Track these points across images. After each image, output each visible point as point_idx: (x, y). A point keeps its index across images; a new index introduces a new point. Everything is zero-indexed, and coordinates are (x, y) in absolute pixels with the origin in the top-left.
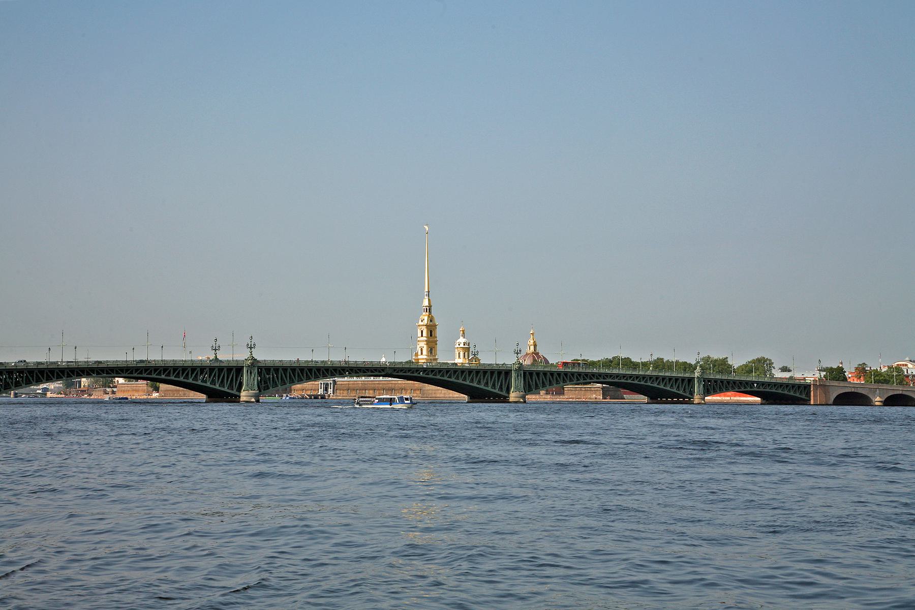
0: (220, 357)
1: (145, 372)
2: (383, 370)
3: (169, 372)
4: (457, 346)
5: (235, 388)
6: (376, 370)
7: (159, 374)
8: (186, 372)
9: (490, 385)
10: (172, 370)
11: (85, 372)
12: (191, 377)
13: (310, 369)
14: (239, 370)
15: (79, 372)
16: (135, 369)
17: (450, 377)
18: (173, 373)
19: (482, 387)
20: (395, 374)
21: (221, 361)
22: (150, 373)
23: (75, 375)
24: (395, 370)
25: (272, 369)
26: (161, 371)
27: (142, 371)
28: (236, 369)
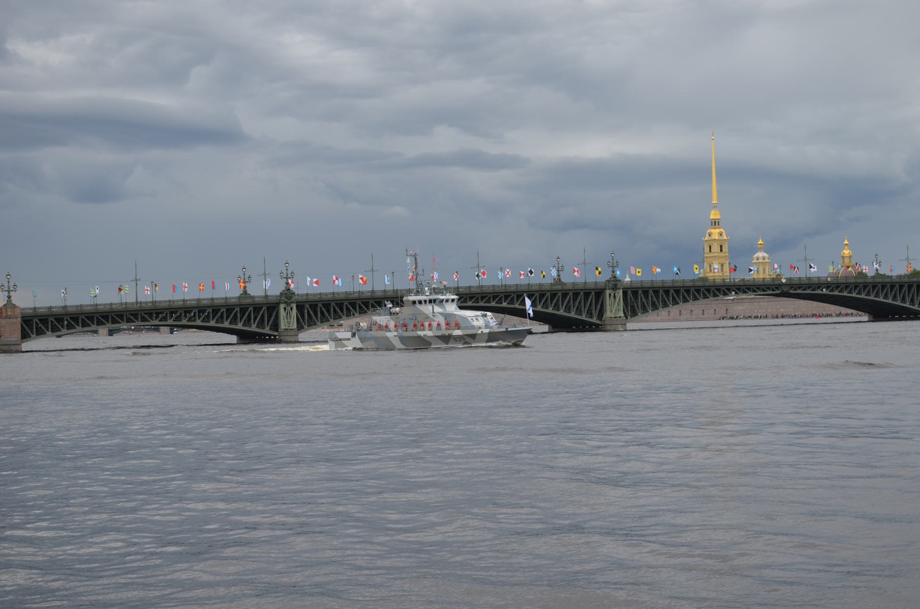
0: (564, 280)
1: (482, 300)
2: (777, 288)
3: (512, 299)
4: (755, 261)
5: (595, 314)
6: (768, 288)
7: (500, 302)
8: (545, 298)
9: (908, 299)
10: (515, 297)
11: (110, 317)
12: (551, 304)
13: (327, 305)
14: (599, 293)
15: (100, 318)
16: (470, 297)
17: (859, 293)
18: (517, 300)
19: (898, 303)
20: (792, 291)
21: (565, 284)
22: (488, 301)
23: (110, 321)
24: (791, 288)
25: (640, 292)
26: (501, 298)
27: (477, 299)
28: (595, 293)
